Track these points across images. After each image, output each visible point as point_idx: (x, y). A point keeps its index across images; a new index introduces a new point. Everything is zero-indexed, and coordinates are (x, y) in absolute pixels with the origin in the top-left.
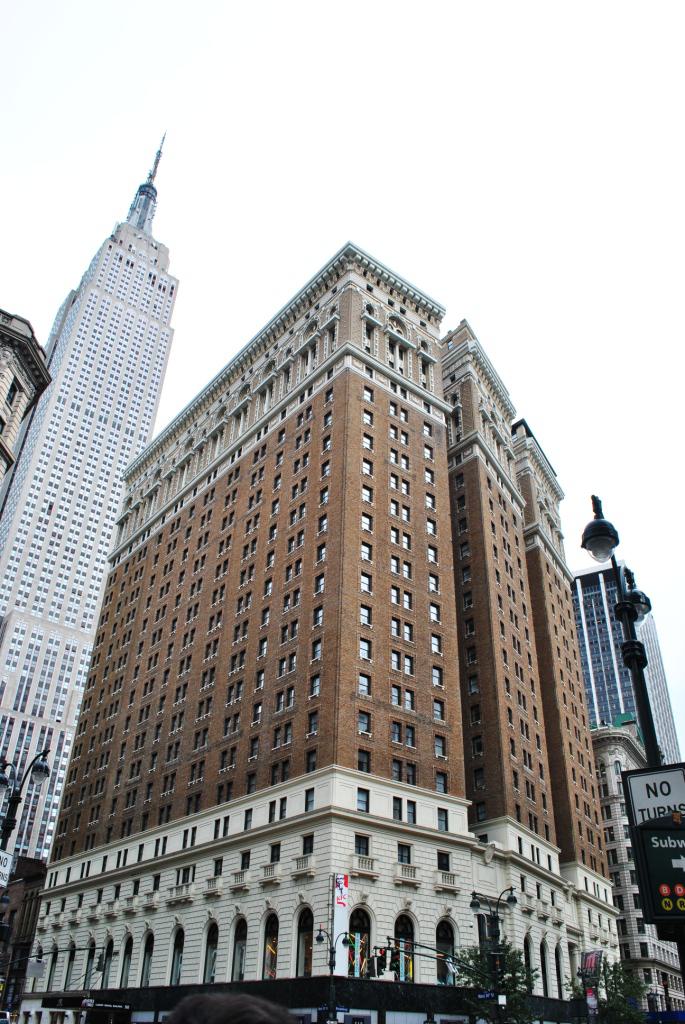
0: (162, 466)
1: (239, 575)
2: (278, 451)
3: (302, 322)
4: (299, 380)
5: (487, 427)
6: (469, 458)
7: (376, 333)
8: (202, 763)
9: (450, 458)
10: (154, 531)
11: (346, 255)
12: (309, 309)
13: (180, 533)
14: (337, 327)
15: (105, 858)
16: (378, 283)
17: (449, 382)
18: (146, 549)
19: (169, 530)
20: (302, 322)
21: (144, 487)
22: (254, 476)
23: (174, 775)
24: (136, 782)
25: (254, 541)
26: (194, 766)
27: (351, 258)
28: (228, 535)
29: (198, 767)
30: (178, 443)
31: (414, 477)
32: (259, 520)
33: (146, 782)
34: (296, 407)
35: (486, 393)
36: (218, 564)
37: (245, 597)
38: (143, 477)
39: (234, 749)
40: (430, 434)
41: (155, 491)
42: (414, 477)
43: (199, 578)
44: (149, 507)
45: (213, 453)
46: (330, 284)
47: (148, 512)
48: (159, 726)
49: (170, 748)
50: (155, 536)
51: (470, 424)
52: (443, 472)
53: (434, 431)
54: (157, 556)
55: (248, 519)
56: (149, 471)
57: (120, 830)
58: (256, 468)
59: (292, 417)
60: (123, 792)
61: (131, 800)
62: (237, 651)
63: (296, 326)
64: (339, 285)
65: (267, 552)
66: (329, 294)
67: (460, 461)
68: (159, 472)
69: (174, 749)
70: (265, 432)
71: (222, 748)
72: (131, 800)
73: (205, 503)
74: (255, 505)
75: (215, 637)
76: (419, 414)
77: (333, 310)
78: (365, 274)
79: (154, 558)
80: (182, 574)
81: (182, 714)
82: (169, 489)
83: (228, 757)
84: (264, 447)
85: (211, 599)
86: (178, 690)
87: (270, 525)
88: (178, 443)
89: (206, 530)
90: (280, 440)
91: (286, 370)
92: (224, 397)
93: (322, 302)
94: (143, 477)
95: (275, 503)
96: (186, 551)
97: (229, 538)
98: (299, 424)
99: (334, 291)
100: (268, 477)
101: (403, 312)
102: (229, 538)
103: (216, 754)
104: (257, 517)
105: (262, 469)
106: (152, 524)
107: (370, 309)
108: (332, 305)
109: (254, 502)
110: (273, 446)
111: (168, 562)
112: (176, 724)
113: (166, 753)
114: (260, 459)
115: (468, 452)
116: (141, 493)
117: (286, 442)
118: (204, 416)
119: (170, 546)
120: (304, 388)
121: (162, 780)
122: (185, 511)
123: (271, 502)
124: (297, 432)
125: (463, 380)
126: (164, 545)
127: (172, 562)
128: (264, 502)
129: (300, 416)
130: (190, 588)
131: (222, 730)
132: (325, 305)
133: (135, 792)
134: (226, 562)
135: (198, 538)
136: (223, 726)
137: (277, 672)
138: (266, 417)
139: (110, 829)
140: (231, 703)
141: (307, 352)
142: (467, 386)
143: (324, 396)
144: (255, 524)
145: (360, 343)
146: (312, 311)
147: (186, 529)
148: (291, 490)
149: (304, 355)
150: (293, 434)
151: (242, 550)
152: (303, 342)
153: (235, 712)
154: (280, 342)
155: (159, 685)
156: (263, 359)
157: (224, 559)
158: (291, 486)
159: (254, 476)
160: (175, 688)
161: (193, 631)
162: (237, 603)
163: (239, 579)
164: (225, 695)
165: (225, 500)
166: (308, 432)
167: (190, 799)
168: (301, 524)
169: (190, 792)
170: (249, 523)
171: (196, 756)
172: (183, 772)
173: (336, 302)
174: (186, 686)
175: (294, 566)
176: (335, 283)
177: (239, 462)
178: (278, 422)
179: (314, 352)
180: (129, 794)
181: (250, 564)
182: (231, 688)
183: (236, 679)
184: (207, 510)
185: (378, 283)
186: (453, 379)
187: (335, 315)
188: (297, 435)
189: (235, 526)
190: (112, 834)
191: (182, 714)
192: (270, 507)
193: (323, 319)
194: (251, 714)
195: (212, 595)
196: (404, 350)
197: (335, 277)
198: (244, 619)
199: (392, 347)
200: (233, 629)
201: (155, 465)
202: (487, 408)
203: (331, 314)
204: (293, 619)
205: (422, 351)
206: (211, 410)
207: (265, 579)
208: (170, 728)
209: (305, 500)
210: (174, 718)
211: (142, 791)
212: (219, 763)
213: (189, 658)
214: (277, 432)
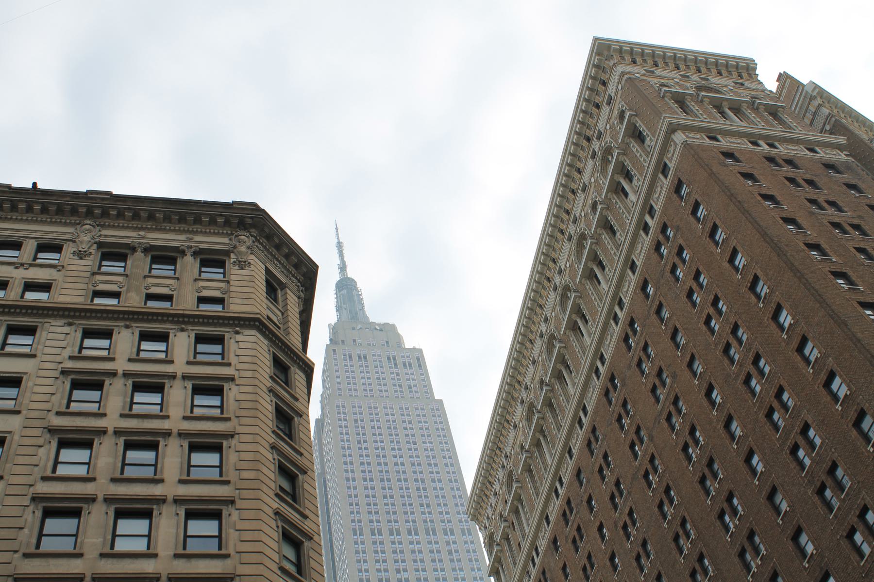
0: (510, 466)
1: (698, 487)
2: (654, 307)
10: (543, 544)
11: (599, 54)
13: (580, 514)
14: (639, 123)
18: (544, 573)
19: (563, 523)
20: (590, 165)
21: (500, 507)
28: (648, 458)
30: (515, 426)
36: (657, 501)
37: (725, 506)
38: (493, 500)
41: (518, 498)
43: (640, 542)
44: (520, 524)
45: (567, 395)
47: (522, 530)
50: (548, 547)
54: (564, 568)
55: (665, 415)
56: (497, 486)
59: (648, 258)
63: (586, 177)
65: (720, 426)
68: (510, 475)
73: (592, 453)
79: (561, 572)
80: (612, 558)
82: (534, 482)
85: (675, 552)
87: (703, 392)
88: (515, 426)
89: (613, 480)
90: (647, 296)
92: (543, 327)
94: (493, 500)
96: (600, 528)
106: (536, 537)
111: (585, 561)
116: (501, 516)
118: (531, 368)
119: (574, 541)
120: (642, 215)
122: (570, 484)
123: (684, 366)
124: (665, 265)
126: (565, 546)
127: (589, 557)
128: (674, 376)
130: (635, 564)
135: (607, 498)
137: (854, 556)
146: (596, 145)
147: (585, 504)
154: (576, 211)
156: (567, 245)
157: (662, 489)
162: (718, 523)
165: (616, 425)
168: (748, 350)
184: (601, 456)
192: (687, 373)
200: (736, 560)
201: (501, 474)
204: (826, 466)
206: (536, 353)
209: (732, 320)
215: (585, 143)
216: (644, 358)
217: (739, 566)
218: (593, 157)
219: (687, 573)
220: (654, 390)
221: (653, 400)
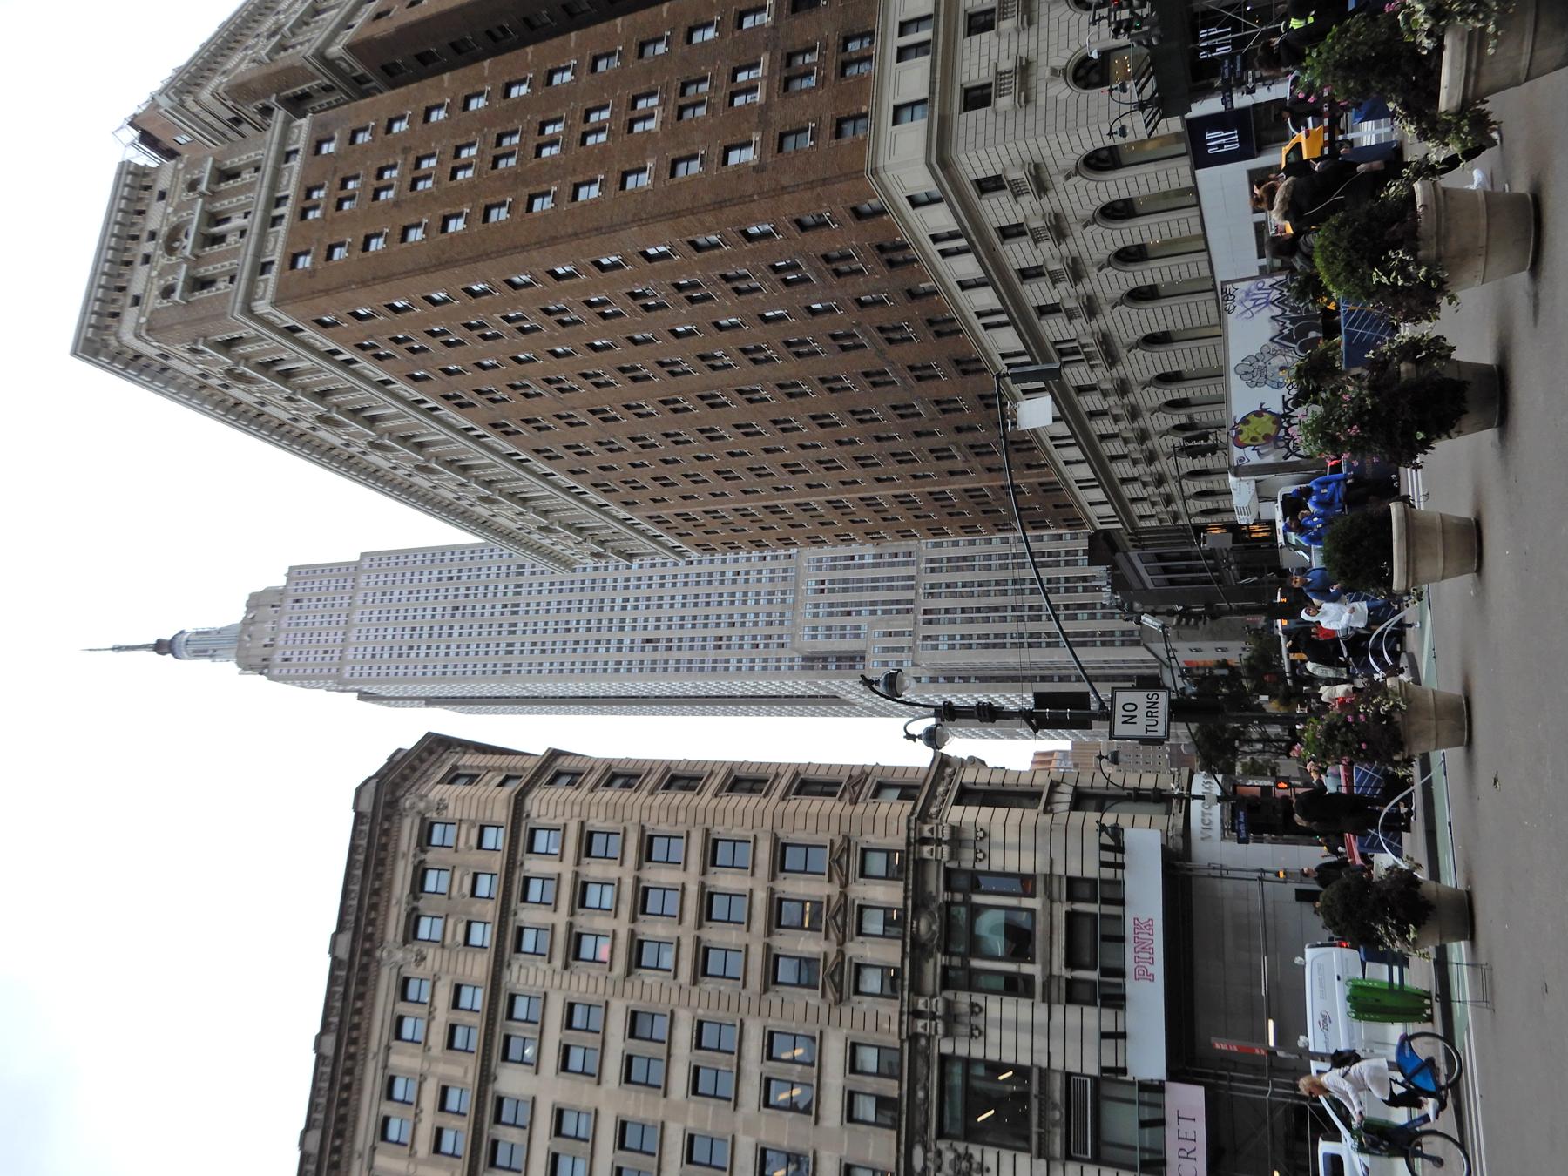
2: (444, 376)
3: (238, 392)
4: (330, 375)
5: (293, 41)
6: (348, 57)
7: (205, 271)
8: (912, 368)
9: (365, 94)
11: (96, 354)
12: (212, 388)
15: (1067, 463)
16: (122, 289)
17: (245, 128)
22: (493, 401)
23: (938, 402)
24: (959, 448)
25: (585, 376)
26: (919, 378)
27: (98, 345)
29: (919, 373)
31: (406, 151)
32: (553, 377)
33: (955, 437)
34: (365, 365)
35: (239, 55)
39: (881, 329)
40: (330, 140)
42: (406, 151)
46: (157, 367)
48: (878, 439)
49: (902, 416)
51: (292, 74)
52: (387, 99)
53: (324, 135)
55: (557, 393)
57: (1027, 454)
58: (480, 401)
59: (385, 369)
60: (976, 462)
61: (984, 450)
62: (745, 360)
64: (149, 350)
65: (593, 354)
66: (174, 363)
67: (363, 76)
69: (903, 412)
70: (424, 401)
71: (885, 346)
72: (984, 450)
74: (534, 389)
75: (736, 395)
76: (306, 166)
77: (194, 351)
78: (115, 315)
81: (853, 413)
83: (897, 336)
84: (447, 397)
86: (822, 426)
87: (554, 359)
90: (425, 378)
91: (322, 396)
93: (192, 371)
95: (519, 361)
97: (593, 412)
98: (389, 356)
99: (165, 357)
100: (486, 381)
101: (153, 236)
102: (593, 412)
103: (894, 352)
104: (549, 381)
105: (480, 392)
107: (167, 292)
108: (187, 355)
109: (531, 391)
110: (441, 383)
112: (868, 416)
113: (910, 420)
114: (466, 399)
115: (344, 65)
117: (424, 369)
121: (947, 415)
123: (519, 367)
125: (230, 103)
128: (524, 377)
129: (378, 357)
131: (860, 352)
132: (193, 365)
133: (972, 447)
134: (628, 407)
136: (853, 353)
138: (401, 406)
139: (1029, 467)
140: (819, 349)
141: (278, 372)
142: (240, 91)
143: (331, 330)
144: (560, 381)
145: (227, 295)
146: (214, 382)
148: (491, 342)
149: (286, 376)
150: (408, 360)
151: (603, 389)
152: (269, 383)
153: (830, 341)
155: (825, 453)
158: (486, 344)
159: (493, 401)
160: (821, 431)
161: (738, 427)
163: (645, 383)
164: (810, 360)
166: (396, 340)
167: (965, 372)
169: (955, 374)
170: (562, 390)
171: (903, 379)
172: (930, 389)
173: (180, 349)
174: (814, 418)
175: (598, 310)
176: (150, 358)
177: (483, 427)
178: (400, 386)
179: (274, 362)
180: (977, 454)
181: (618, 374)
182: (798, 355)
183: (783, 350)
185: (122, 289)
186: (237, 121)
187: (201, 347)
188: (408, 354)
189: (574, 408)
190: (1035, 463)
191: (853, 413)
193: (217, 362)
194: (826, 317)
195: (679, 414)
196: (216, 219)
197: (142, 361)
198: (698, 361)
199: (219, 239)
200: (716, 373)
202: (263, 48)
203: (202, 352)
205: (203, 187)
207: (631, 346)
208: (876, 424)
210: (861, 421)
211: (969, 438)
212: (906, 345)
213: (775, 422)
214: (416, 384)
215: (204, 392)
216: (490, 396)
217: (724, 372)
218: (226, 386)
219: (709, 409)
220: (527, 396)
221: (537, 399)
